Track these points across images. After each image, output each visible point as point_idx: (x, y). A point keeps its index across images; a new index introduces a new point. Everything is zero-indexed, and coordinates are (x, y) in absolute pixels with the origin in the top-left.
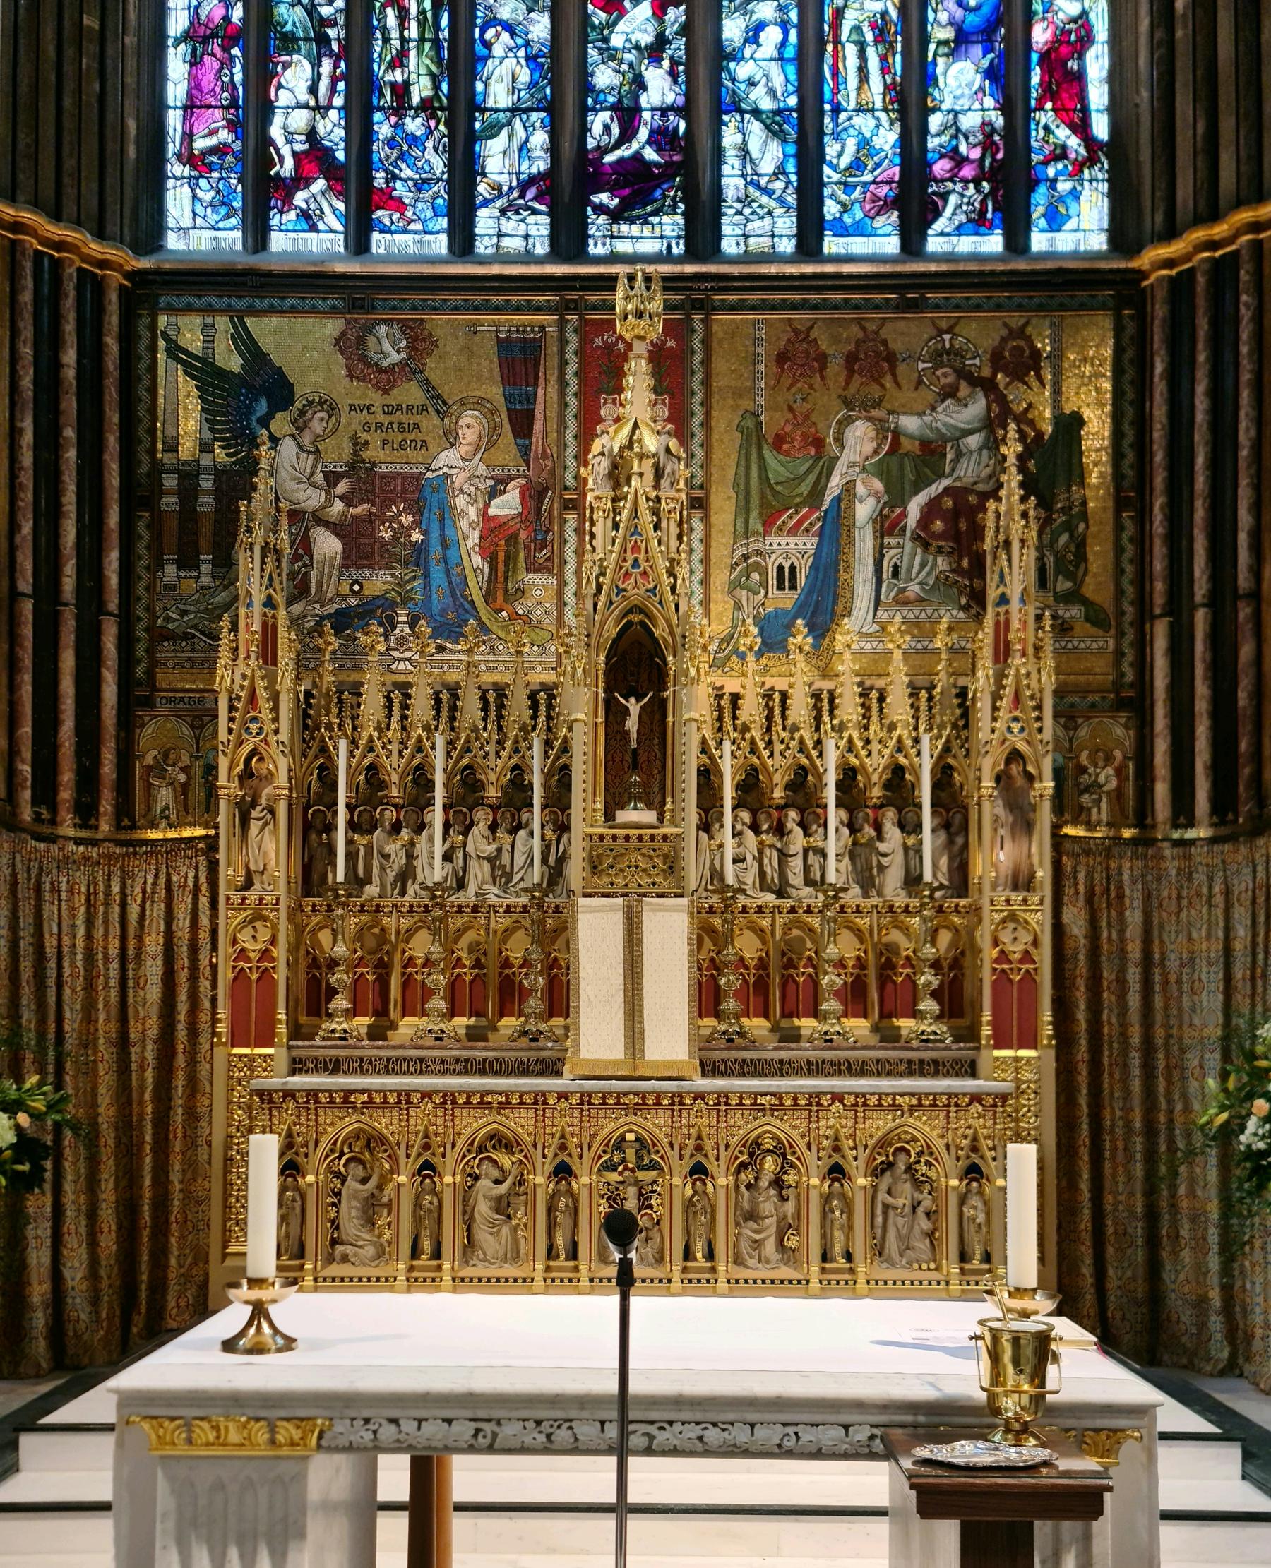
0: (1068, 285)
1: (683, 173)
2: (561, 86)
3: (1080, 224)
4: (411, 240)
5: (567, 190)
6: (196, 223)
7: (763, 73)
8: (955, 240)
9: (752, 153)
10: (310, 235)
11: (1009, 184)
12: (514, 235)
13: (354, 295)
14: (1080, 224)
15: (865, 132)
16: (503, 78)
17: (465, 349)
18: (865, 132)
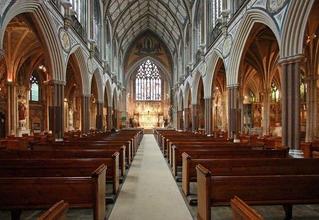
0: (160, 101)
1: (150, 98)
2: (147, 95)
3: (160, 99)
4: (143, 99)
5: (147, 98)
6: (137, 99)
7: (152, 95)
8: (157, 100)
9: (152, 98)
10: (140, 99)
11: (158, 99)
12: (145, 99)
13: (141, 101)
14: (160, 99)
15: (154, 97)
16: (145, 95)
17: (144, 103)
18: (154, 97)
